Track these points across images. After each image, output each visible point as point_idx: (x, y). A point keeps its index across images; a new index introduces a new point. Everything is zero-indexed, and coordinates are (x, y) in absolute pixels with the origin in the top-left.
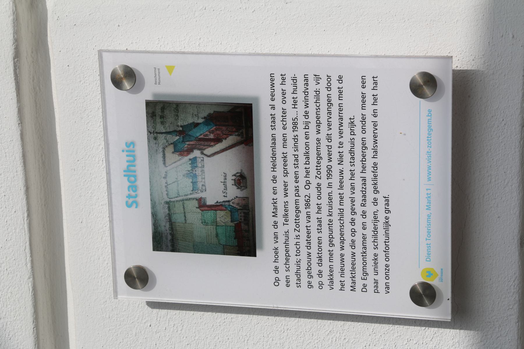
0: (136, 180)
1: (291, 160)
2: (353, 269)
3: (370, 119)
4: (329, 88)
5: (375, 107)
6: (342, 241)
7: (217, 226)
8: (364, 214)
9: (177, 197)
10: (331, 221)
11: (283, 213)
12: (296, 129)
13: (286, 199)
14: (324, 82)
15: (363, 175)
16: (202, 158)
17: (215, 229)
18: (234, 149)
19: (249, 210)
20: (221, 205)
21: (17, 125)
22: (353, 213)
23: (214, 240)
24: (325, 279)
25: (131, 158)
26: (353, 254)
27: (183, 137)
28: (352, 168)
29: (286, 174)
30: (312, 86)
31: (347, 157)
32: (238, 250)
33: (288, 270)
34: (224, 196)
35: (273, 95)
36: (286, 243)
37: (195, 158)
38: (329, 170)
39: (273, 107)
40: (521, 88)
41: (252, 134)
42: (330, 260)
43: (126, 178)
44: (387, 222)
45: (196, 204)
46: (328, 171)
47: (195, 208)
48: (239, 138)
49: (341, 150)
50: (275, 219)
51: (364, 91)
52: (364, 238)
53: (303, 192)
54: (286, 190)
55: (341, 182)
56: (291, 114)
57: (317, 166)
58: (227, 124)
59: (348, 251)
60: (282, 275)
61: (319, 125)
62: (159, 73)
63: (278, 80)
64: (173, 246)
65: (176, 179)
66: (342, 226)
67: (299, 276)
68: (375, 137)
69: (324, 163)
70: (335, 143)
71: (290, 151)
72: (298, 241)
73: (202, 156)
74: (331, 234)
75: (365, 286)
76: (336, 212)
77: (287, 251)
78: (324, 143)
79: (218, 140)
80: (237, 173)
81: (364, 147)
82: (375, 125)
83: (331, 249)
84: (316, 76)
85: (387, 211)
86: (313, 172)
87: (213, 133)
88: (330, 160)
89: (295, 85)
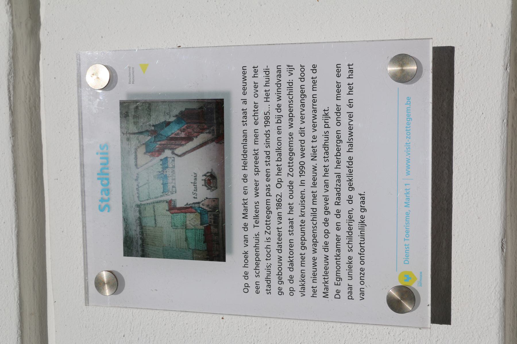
2: (326, 273)
3: (345, 109)
4: (302, 79)
5: (350, 97)
6: (315, 243)
7: (186, 229)
8: (338, 214)
9: (148, 200)
10: (303, 222)
11: (254, 214)
12: (268, 124)
13: (257, 200)
14: (297, 73)
15: (337, 171)
16: (173, 159)
17: (184, 233)
20: (191, 207)
21: (9, 138)
23: (184, 244)
24: (297, 286)
25: (105, 161)
26: (326, 257)
27: (155, 137)
28: (326, 164)
30: (285, 78)
31: (321, 152)
32: (207, 255)
33: (258, 276)
34: (194, 198)
35: (244, 89)
36: (256, 247)
37: (166, 158)
38: (302, 166)
39: (245, 102)
40: (502, 79)
41: (223, 131)
43: (100, 181)
44: (362, 222)
45: (166, 206)
46: (301, 168)
49: (314, 144)
50: (245, 221)
51: (339, 80)
52: (338, 240)
53: (274, 191)
54: (256, 189)
55: (314, 179)
59: (320, 254)
61: (291, 118)
62: (133, 72)
64: (143, 251)
65: (148, 181)
66: (315, 227)
67: (269, 282)
68: (350, 129)
69: (297, 159)
70: (308, 138)
71: (261, 147)
72: (268, 244)
73: (174, 156)
74: (303, 236)
75: (338, 292)
76: (308, 211)
77: (257, 255)
78: (297, 137)
79: (189, 139)
80: (208, 173)
81: (339, 140)
82: (351, 117)
83: (303, 252)
84: (289, 66)
85: (363, 209)
86: (285, 169)
87: (184, 131)
88: (303, 156)
89: (267, 76)
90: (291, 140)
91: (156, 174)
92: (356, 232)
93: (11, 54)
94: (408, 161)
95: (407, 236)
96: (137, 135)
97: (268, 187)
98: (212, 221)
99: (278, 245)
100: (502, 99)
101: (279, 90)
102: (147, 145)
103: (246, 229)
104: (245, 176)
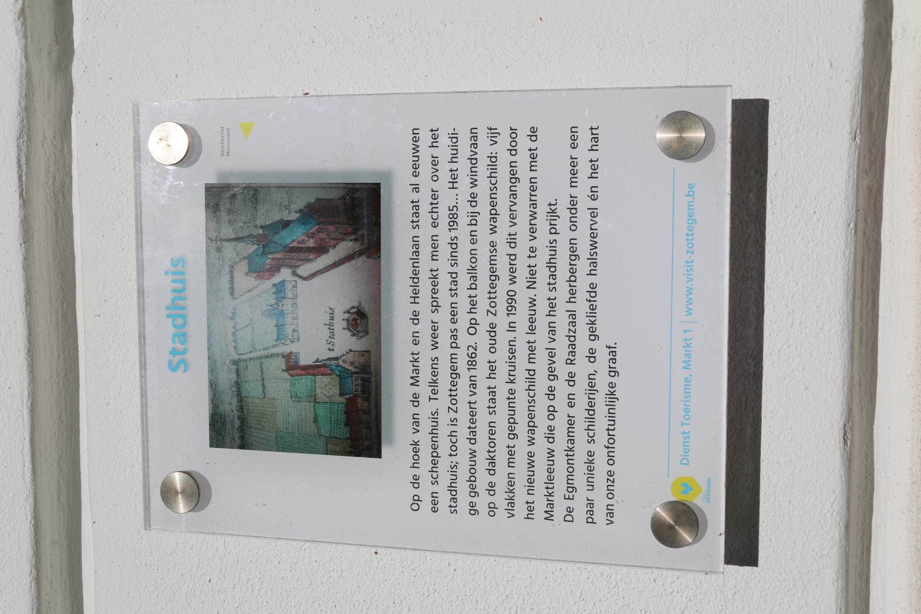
0: (185, 324)
1: (444, 282)
2: (550, 479)
3: (584, 203)
4: (513, 151)
5: (593, 182)
6: (532, 429)
8: (571, 379)
9: (251, 352)
10: (512, 392)
11: (429, 378)
12: (455, 227)
13: (435, 353)
14: (504, 141)
15: (571, 307)
16: (294, 283)
17: (312, 409)
18: (347, 265)
19: (370, 373)
20: (324, 366)
22: (552, 378)
23: (312, 428)
24: (500, 499)
25: (179, 285)
26: (551, 453)
27: (264, 247)
29: (436, 307)
31: (543, 275)
33: (435, 482)
35: (415, 167)
36: (433, 433)
37: (283, 282)
38: (511, 297)
42: (510, 464)
43: (170, 320)
44: (612, 393)
45: (282, 363)
46: (510, 301)
47: (280, 371)
48: (357, 246)
49: (532, 262)
50: (415, 389)
52: (571, 424)
53: (464, 340)
54: (434, 336)
55: (532, 321)
56: (446, 200)
57: (490, 293)
58: (337, 220)
59: (541, 447)
60: (425, 491)
61: (494, 217)
63: (425, 139)
64: (242, 438)
65: (251, 320)
66: (532, 401)
67: (454, 493)
68: (593, 236)
69: (503, 285)
70: (522, 251)
71: (443, 265)
72: (454, 428)
74: (511, 416)
75: (570, 511)
76: (521, 375)
77: (435, 448)
78: (503, 249)
79: (321, 250)
80: (353, 307)
81: (574, 255)
82: (594, 215)
84: (491, 129)
86: (483, 303)
87: (313, 237)
88: (513, 281)
89: (455, 148)
90: (494, 253)
91: (265, 308)
92: (601, 410)
93: (23, 103)
94: (689, 291)
95: (687, 417)
96: (234, 243)
97: (455, 333)
98: (360, 389)
99: (469, 430)
100: (847, 189)
101: (473, 170)
102: (249, 258)
103: (416, 404)
104: (416, 314)
